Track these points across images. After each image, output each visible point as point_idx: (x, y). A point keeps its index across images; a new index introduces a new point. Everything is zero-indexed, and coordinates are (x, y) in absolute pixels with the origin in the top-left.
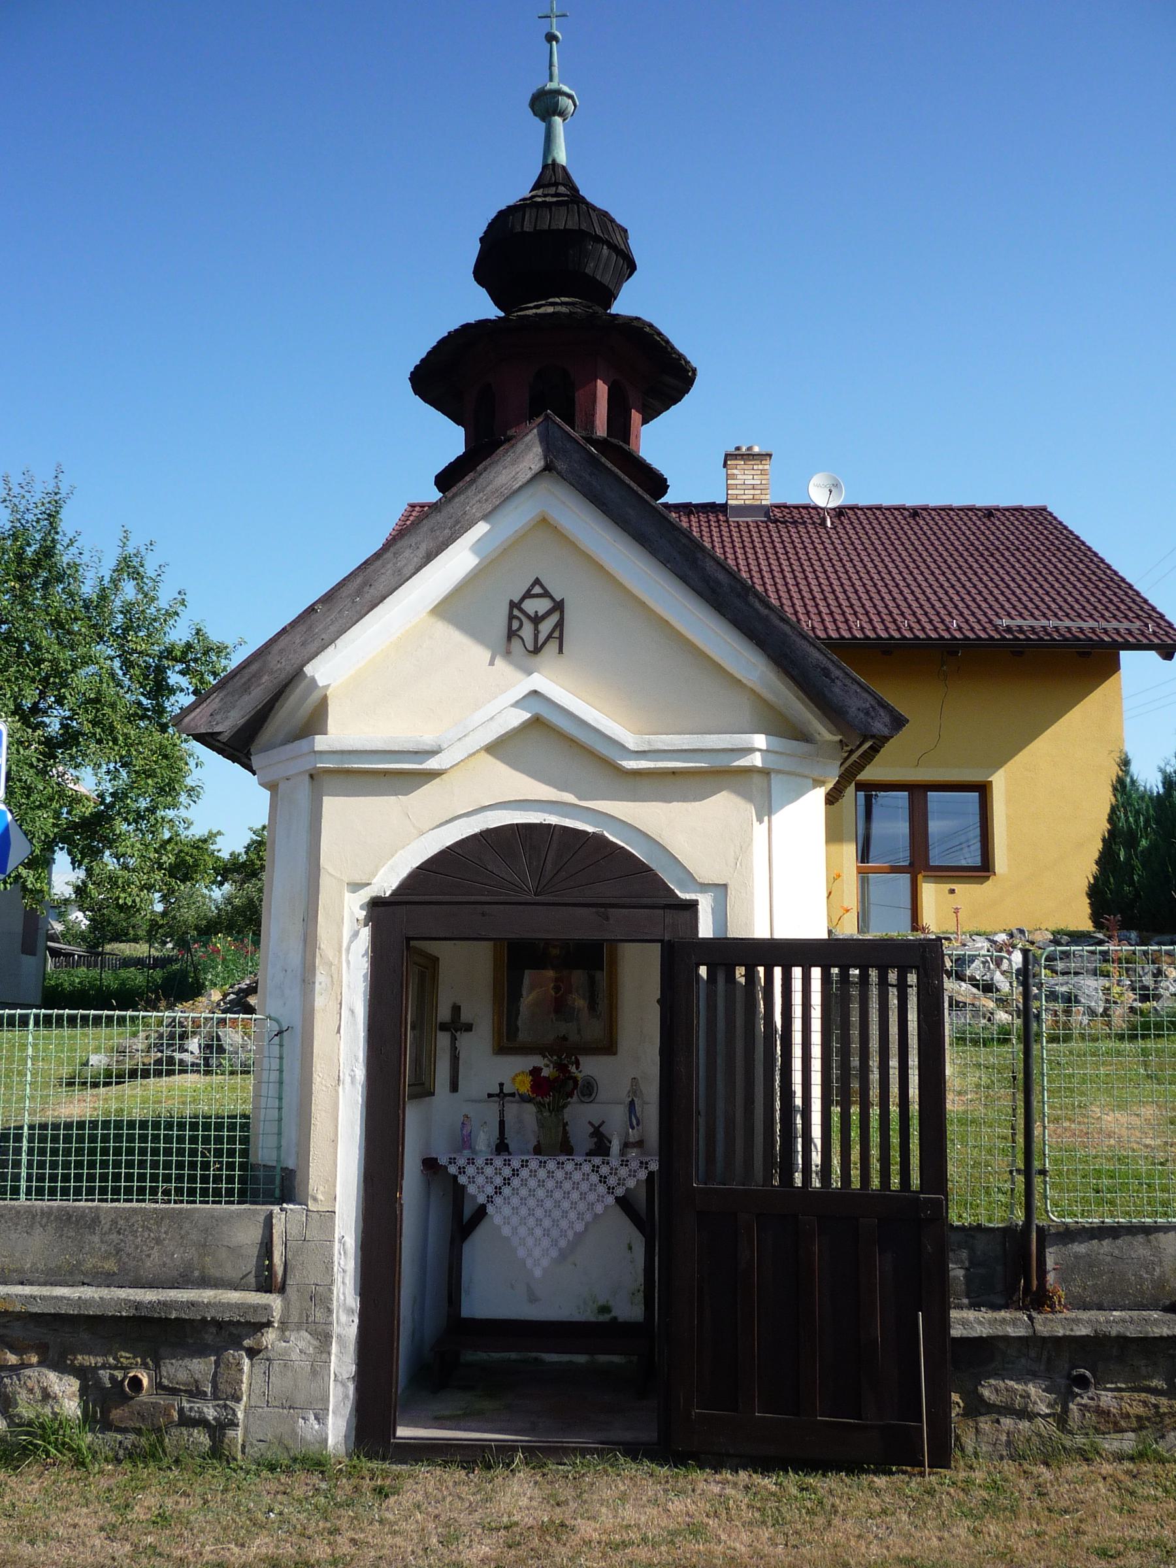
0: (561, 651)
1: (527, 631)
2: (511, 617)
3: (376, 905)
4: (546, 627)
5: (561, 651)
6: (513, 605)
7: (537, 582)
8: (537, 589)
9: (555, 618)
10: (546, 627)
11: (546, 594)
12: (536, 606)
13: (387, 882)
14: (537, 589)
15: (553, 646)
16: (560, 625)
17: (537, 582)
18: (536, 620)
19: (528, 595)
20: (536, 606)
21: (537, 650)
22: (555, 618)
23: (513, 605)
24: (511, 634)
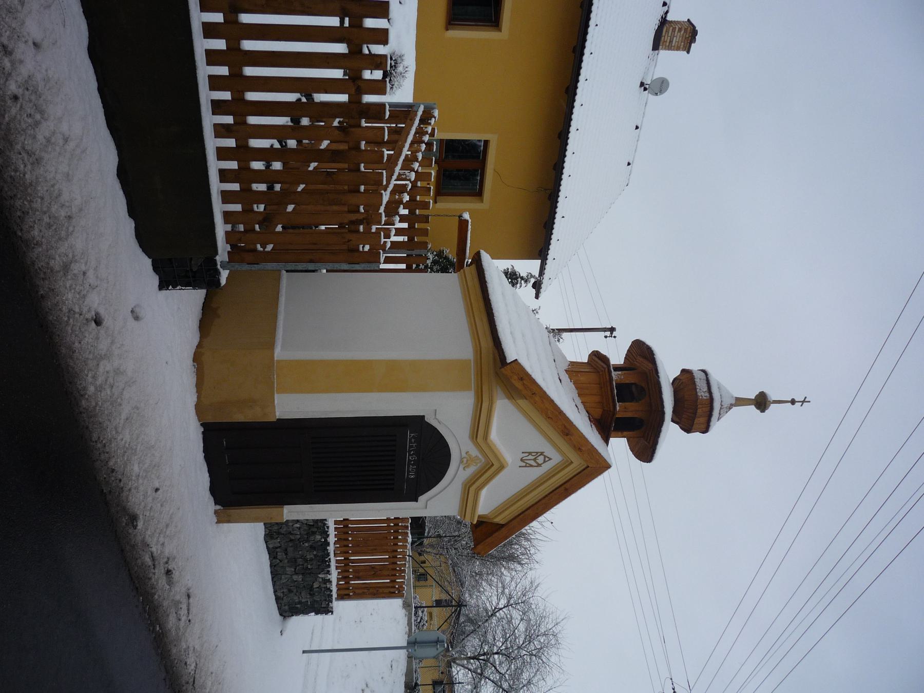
1: (530, 457)
4: (532, 463)
7: (550, 459)
9: (535, 464)
10: (532, 463)
11: (545, 461)
12: (540, 459)
14: (547, 459)
16: (531, 466)
17: (550, 459)
19: (545, 457)
21: (522, 460)
22: (535, 464)
23: (542, 454)
24: (530, 453)
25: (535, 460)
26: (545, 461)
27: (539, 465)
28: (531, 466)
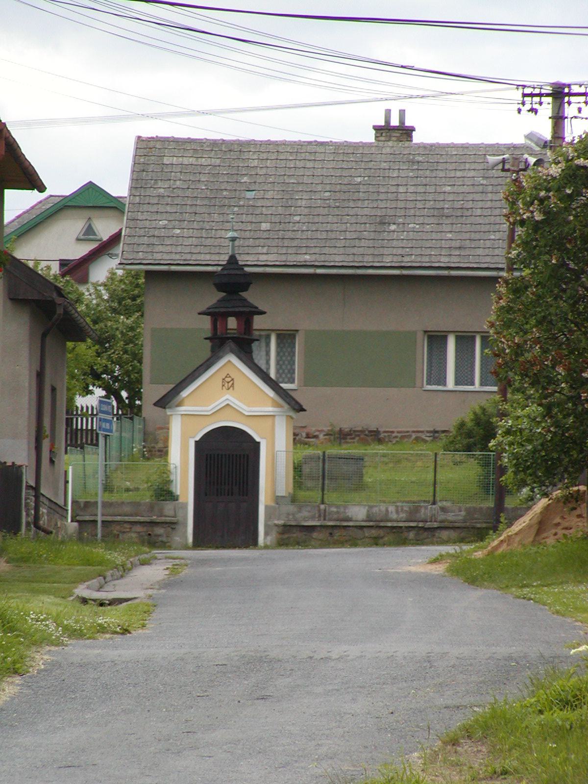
0: (233, 389)
2: (223, 382)
3: (196, 442)
4: (230, 384)
5: (233, 389)
6: (224, 379)
7: (228, 374)
8: (228, 376)
9: (232, 382)
10: (230, 384)
11: (230, 377)
12: (228, 379)
13: (197, 439)
14: (228, 376)
15: (232, 388)
16: (233, 384)
17: (228, 374)
18: (228, 382)
19: (226, 377)
20: (228, 379)
21: (229, 389)
22: (232, 382)
24: (223, 386)
25: (228, 382)
26: (230, 377)
27: (233, 380)
28: (233, 384)
